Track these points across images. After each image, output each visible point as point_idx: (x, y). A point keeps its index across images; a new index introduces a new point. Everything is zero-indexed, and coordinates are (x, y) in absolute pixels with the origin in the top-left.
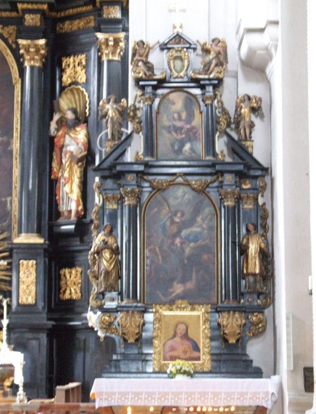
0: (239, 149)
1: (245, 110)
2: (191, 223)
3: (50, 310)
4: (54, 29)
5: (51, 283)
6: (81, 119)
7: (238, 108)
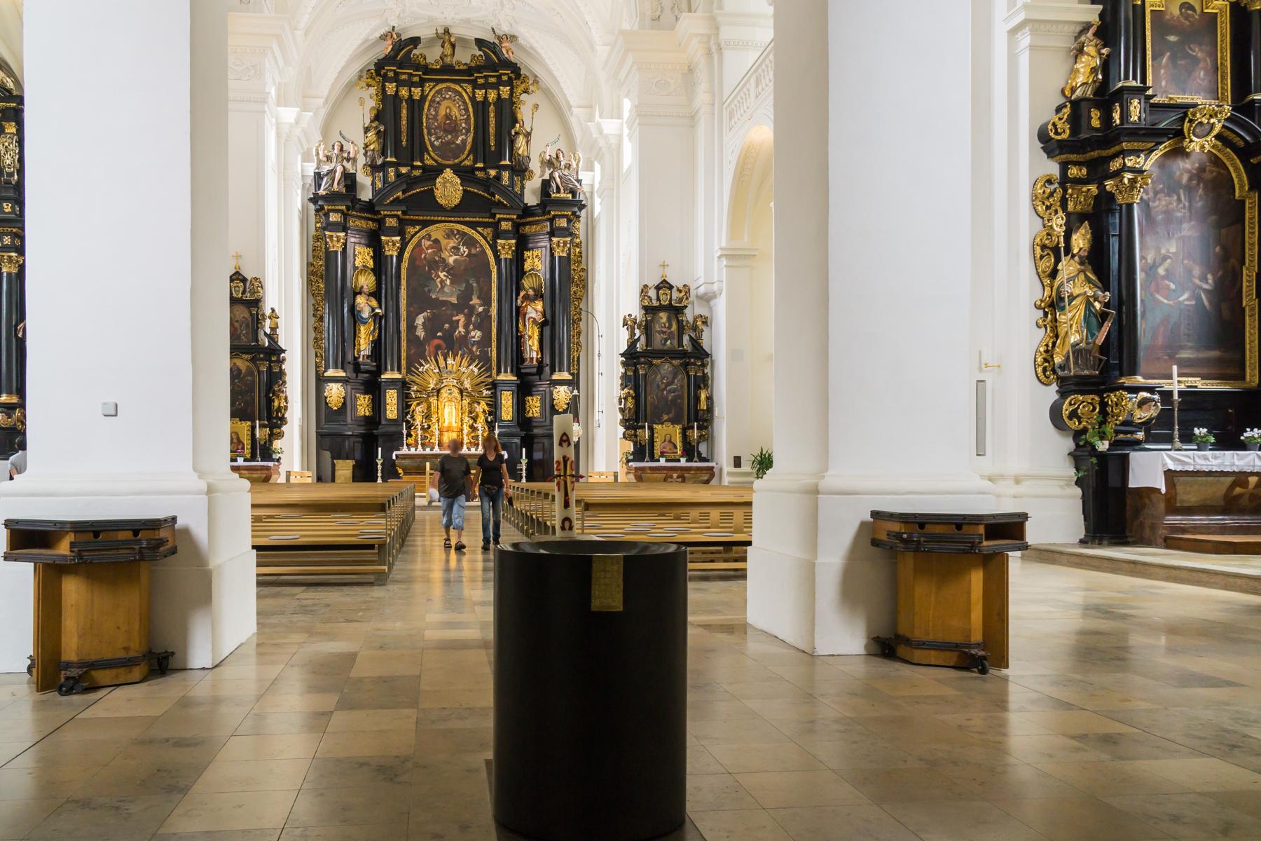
0: (696, 343)
1: (699, 323)
2: (672, 383)
3: (519, 424)
4: (518, 231)
5: (520, 406)
6: (539, 295)
7: (695, 320)
